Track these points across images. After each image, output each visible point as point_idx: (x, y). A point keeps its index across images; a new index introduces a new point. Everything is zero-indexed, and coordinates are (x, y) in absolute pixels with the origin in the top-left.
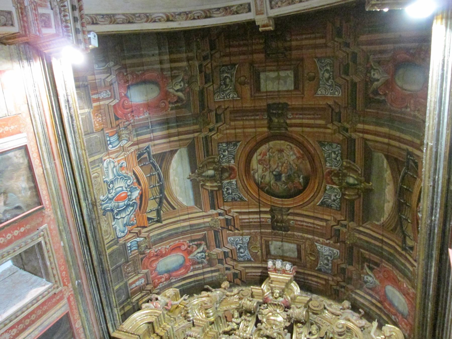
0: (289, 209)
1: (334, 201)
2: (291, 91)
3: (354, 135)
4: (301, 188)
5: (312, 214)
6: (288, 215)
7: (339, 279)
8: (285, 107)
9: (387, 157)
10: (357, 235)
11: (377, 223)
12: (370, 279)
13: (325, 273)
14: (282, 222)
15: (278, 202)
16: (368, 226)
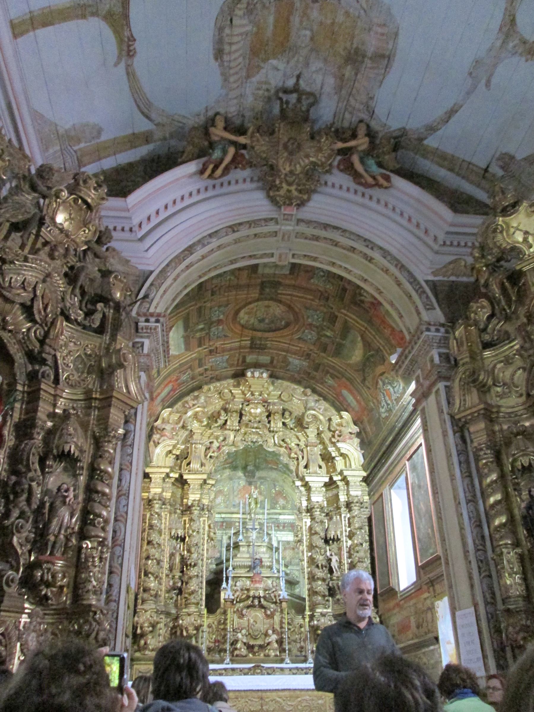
3: (336, 313)
5: (288, 342)
8: (279, 283)
10: (326, 361)
13: (292, 371)
14: (261, 344)
15: (259, 334)
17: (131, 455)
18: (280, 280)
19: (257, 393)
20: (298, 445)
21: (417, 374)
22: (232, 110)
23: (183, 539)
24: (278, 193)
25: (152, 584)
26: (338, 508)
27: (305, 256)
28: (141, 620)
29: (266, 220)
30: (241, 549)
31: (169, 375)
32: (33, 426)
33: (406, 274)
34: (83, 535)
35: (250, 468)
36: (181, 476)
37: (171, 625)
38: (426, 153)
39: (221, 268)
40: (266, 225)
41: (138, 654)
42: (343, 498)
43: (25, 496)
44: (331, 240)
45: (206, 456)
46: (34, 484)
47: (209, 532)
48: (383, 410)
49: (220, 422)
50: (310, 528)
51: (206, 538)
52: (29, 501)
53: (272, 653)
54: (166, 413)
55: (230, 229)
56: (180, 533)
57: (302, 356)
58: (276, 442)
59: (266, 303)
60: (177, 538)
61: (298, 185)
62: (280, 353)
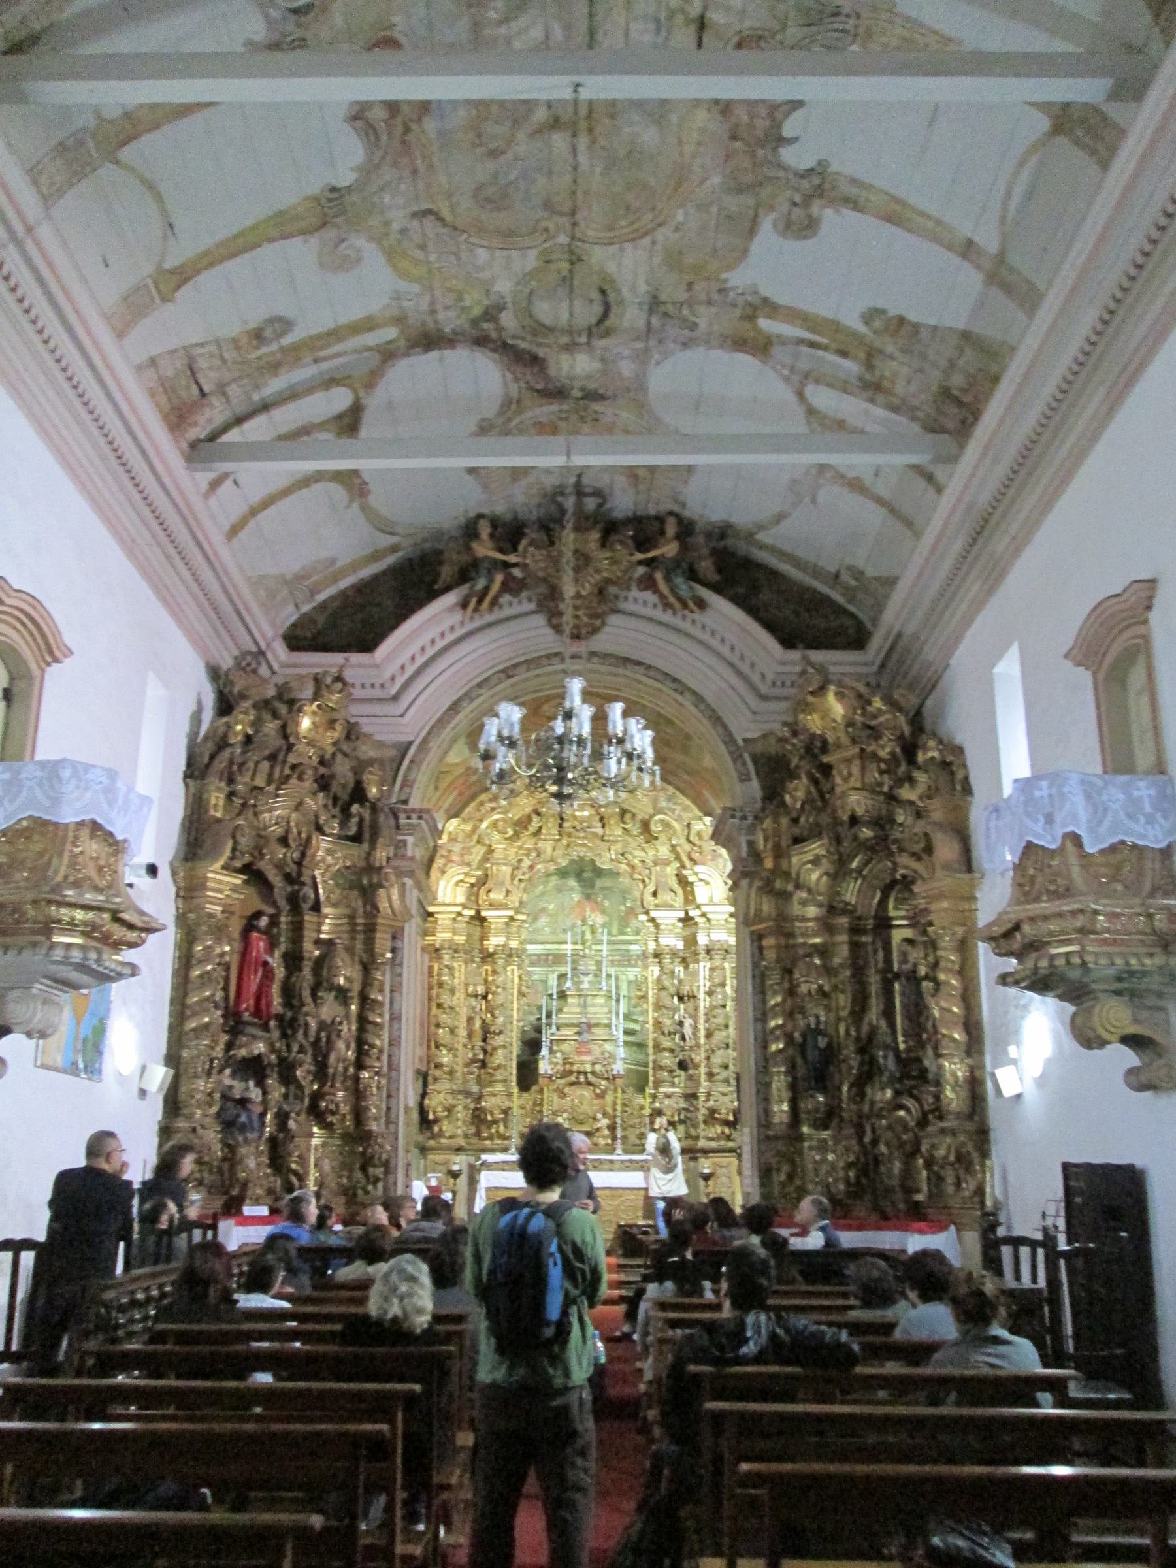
17: (400, 975)
22: (500, 508)
23: (485, 997)
25: (445, 1058)
26: (696, 954)
28: (433, 1104)
29: (548, 657)
30: (570, 1000)
31: (453, 782)
32: (301, 959)
33: (721, 731)
34: (360, 1065)
35: (587, 875)
36: (478, 912)
37: (472, 1106)
38: (762, 546)
41: (432, 1143)
42: (702, 940)
43: (301, 1031)
45: (513, 879)
46: (309, 1019)
47: (520, 985)
49: (532, 829)
50: (659, 980)
51: (515, 992)
52: (306, 1034)
53: (602, 1142)
54: (453, 825)
55: (503, 675)
56: (481, 989)
60: (476, 996)
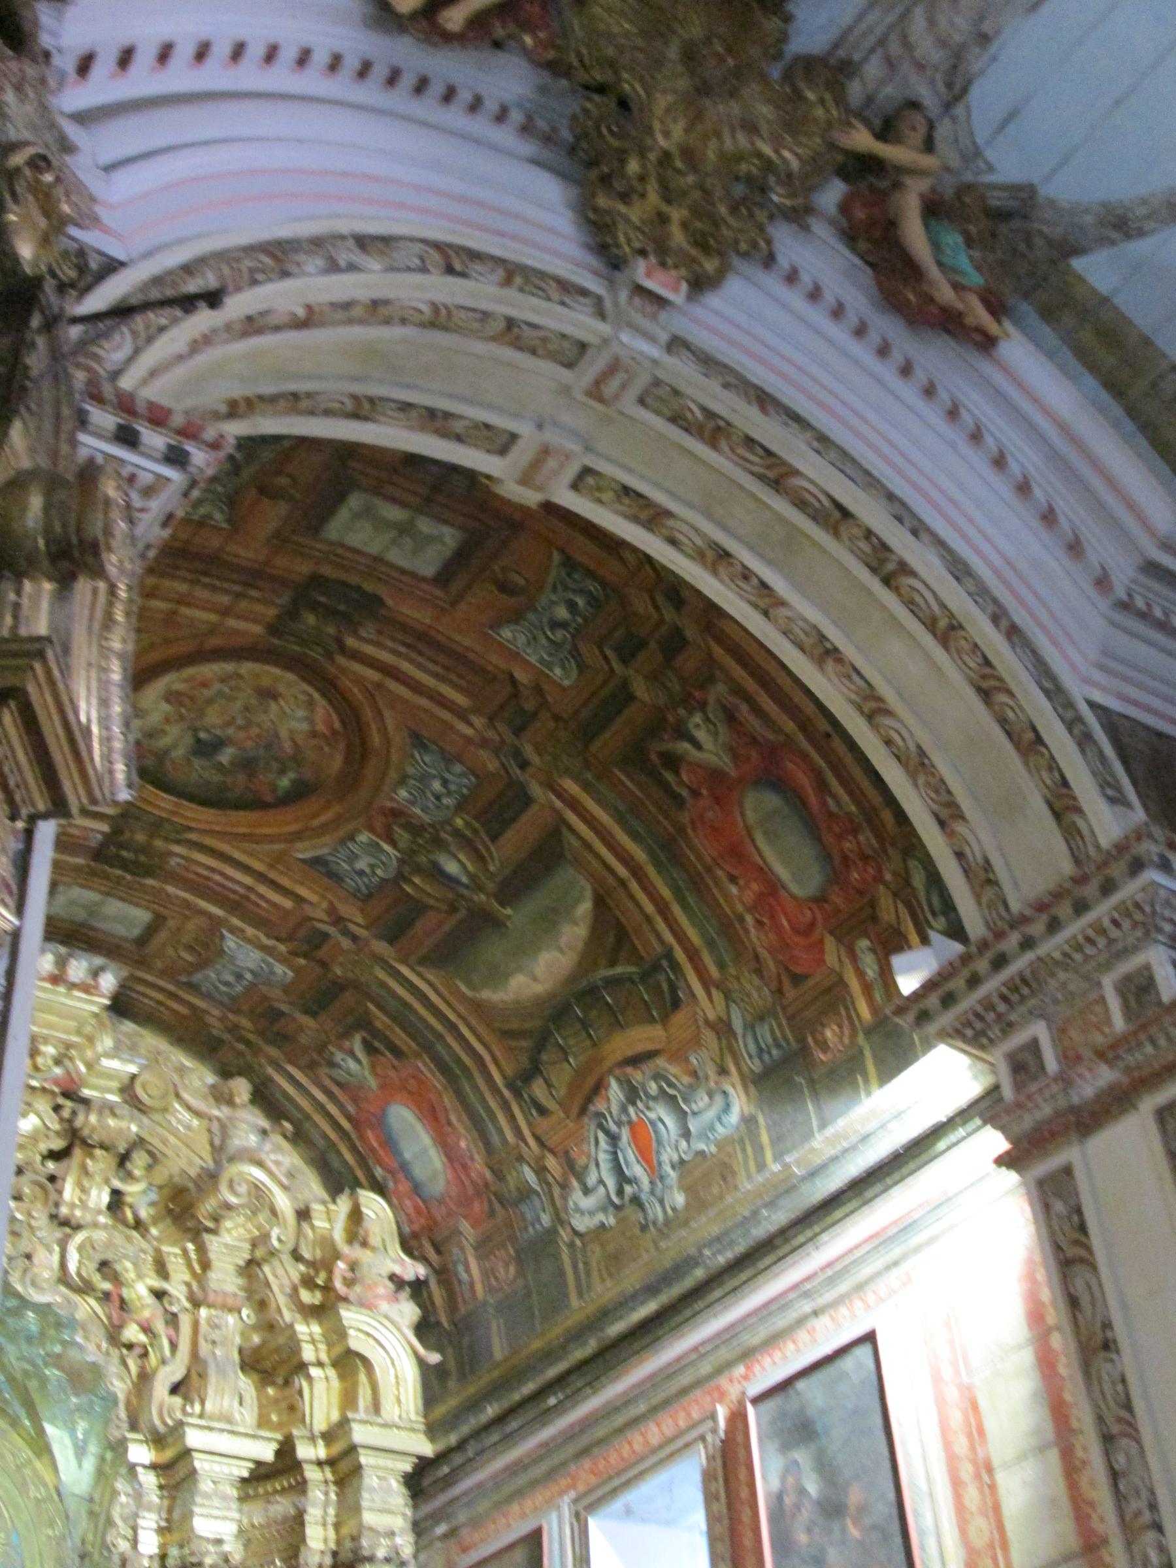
0: (189, 829)
1: (361, 873)
2: (424, 579)
3: (536, 790)
4: (269, 798)
5: (259, 866)
6: (178, 842)
7: (245, 1022)
8: (371, 605)
9: (600, 902)
10: (382, 975)
11: (463, 988)
12: (352, 1065)
13: (207, 996)
16: (431, 977)
18: (382, 591)
19: (50, 1050)
20: (159, 1295)
21: (1019, 1038)
24: (622, 208)
27: (626, 490)
39: (312, 413)
40: (563, 303)
44: (768, 453)
48: (587, 1203)
55: (435, 256)
57: (290, 938)
58: (72, 1267)
59: (271, 673)
61: (696, 212)
62: (203, 904)
